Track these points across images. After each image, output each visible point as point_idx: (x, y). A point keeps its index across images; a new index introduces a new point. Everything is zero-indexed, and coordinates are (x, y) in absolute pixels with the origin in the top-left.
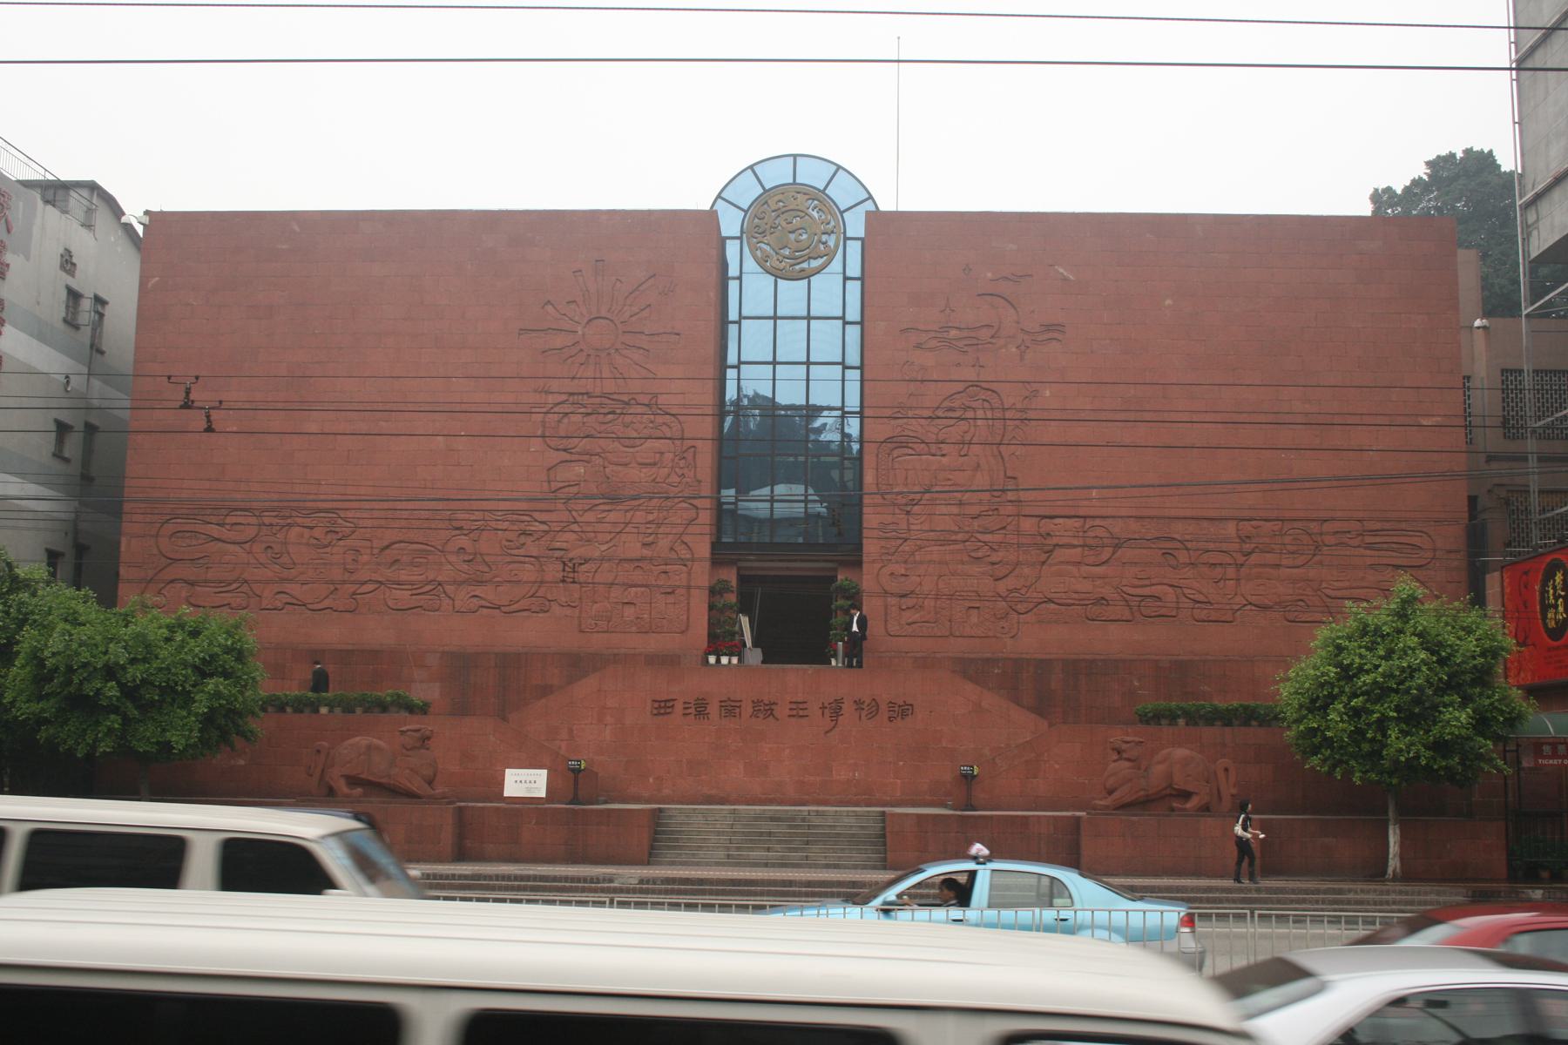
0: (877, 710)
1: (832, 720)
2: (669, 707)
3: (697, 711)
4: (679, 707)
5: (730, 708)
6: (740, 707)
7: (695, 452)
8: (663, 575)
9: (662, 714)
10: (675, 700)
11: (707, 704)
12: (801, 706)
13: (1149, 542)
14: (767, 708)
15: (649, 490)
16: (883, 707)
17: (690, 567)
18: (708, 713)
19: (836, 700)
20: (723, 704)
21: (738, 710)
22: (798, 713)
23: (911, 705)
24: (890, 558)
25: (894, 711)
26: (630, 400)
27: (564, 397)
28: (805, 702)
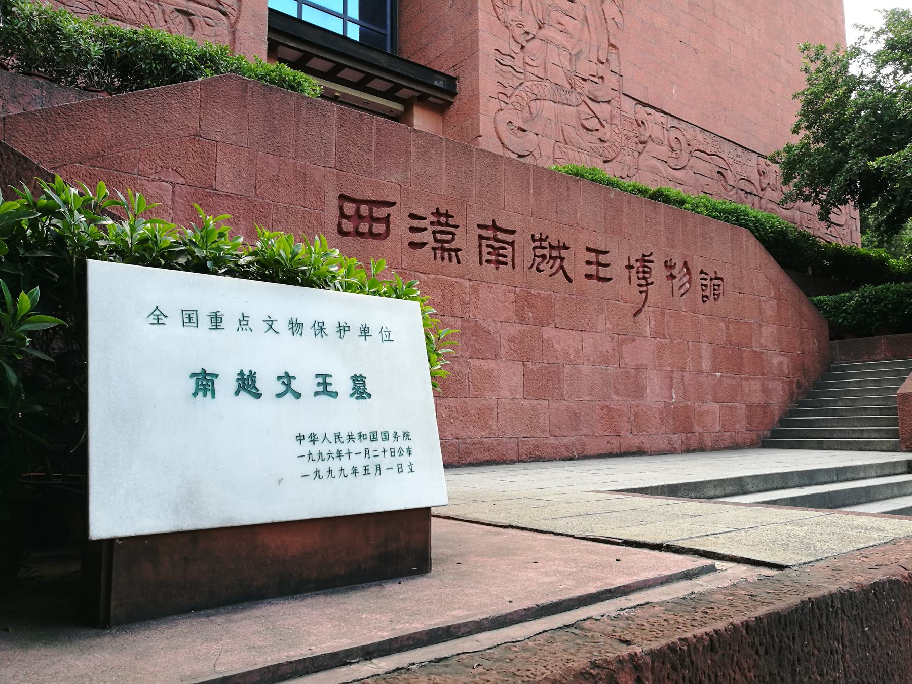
0: (689, 282)
1: (641, 292)
2: (378, 220)
3: (436, 240)
4: (400, 224)
5: (497, 245)
6: (512, 244)
8: (181, 18)
9: (359, 234)
10: (394, 204)
11: (457, 227)
12: (602, 258)
13: (708, 157)
14: (555, 253)
16: (696, 276)
17: (233, 19)
18: (457, 250)
19: (644, 256)
20: (485, 233)
21: (509, 248)
22: (598, 270)
23: (721, 279)
24: (506, 100)
25: (706, 286)
28: (606, 252)
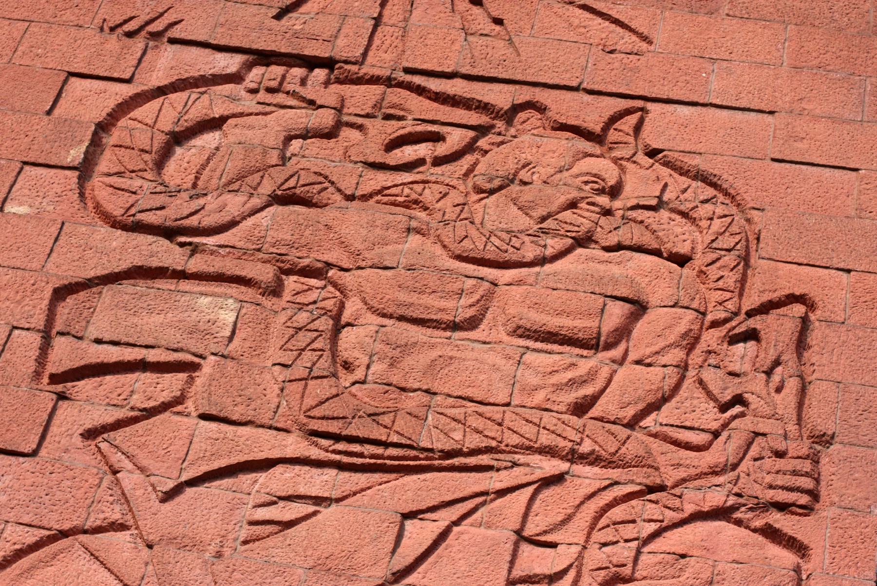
7: (805, 321)
15: (545, 439)
26: (517, 108)
27: (230, 63)
